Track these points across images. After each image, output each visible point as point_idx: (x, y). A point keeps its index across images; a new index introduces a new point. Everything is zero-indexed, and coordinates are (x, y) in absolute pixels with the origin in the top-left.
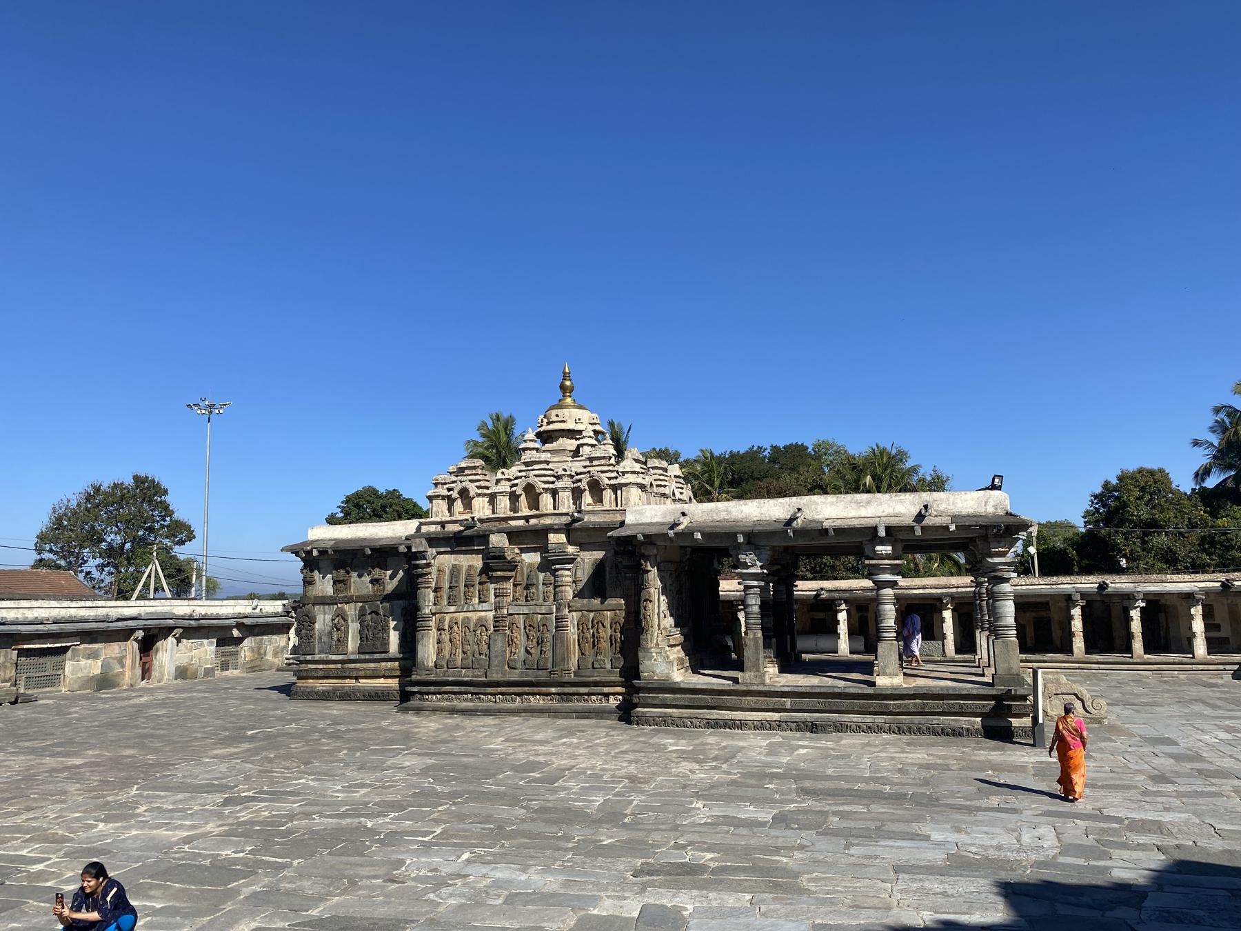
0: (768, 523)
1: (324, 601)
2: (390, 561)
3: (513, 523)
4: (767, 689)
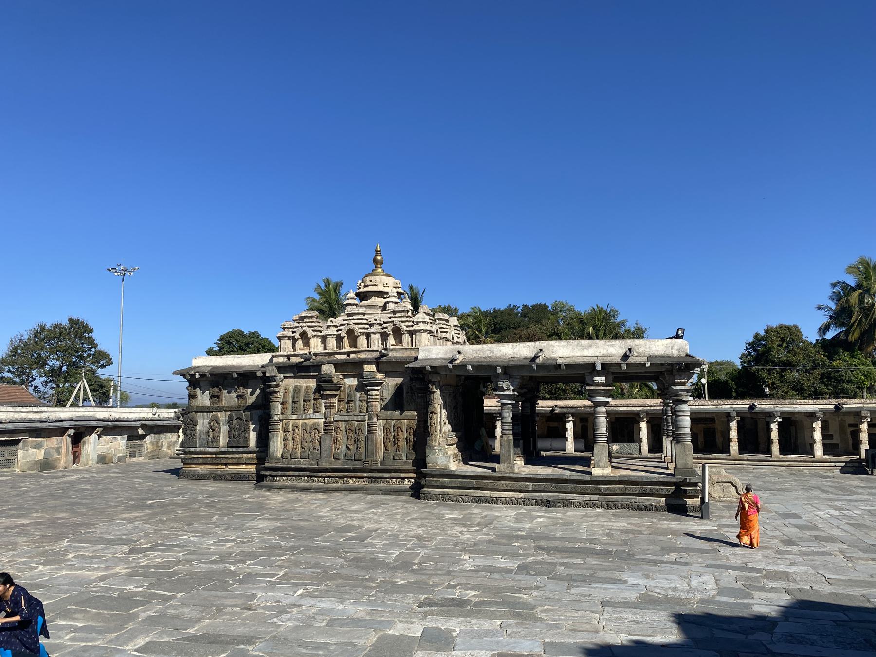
0: (519, 359)
1: (203, 410)
2: (250, 382)
3: (338, 357)
4: (515, 476)
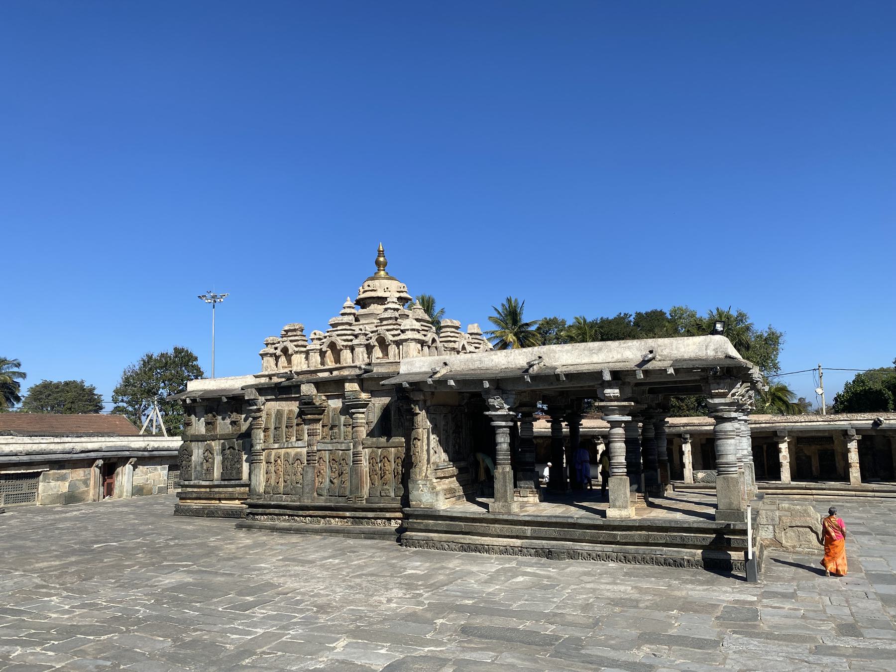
0: (512, 370)
3: (321, 375)
4: (510, 518)
